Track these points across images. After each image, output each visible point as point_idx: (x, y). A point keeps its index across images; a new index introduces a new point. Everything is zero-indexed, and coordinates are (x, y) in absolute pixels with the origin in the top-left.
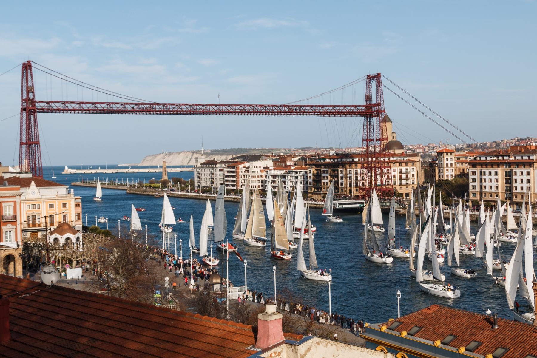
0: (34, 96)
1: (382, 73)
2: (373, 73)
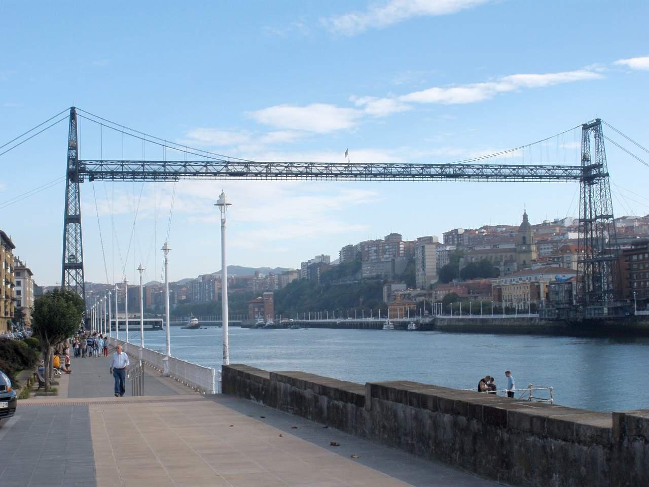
0: (77, 153)
1: (602, 118)
2: (590, 120)
